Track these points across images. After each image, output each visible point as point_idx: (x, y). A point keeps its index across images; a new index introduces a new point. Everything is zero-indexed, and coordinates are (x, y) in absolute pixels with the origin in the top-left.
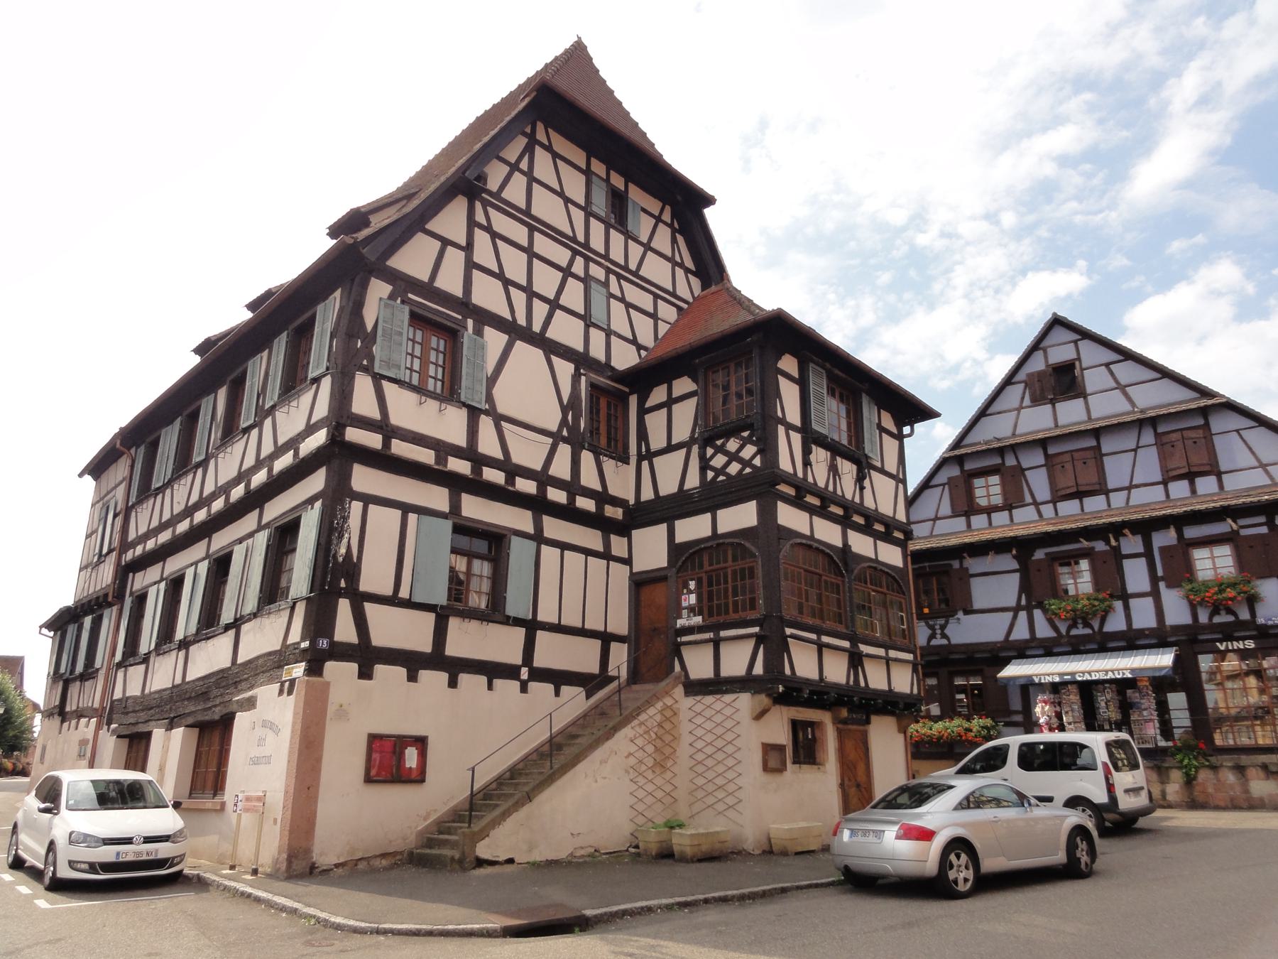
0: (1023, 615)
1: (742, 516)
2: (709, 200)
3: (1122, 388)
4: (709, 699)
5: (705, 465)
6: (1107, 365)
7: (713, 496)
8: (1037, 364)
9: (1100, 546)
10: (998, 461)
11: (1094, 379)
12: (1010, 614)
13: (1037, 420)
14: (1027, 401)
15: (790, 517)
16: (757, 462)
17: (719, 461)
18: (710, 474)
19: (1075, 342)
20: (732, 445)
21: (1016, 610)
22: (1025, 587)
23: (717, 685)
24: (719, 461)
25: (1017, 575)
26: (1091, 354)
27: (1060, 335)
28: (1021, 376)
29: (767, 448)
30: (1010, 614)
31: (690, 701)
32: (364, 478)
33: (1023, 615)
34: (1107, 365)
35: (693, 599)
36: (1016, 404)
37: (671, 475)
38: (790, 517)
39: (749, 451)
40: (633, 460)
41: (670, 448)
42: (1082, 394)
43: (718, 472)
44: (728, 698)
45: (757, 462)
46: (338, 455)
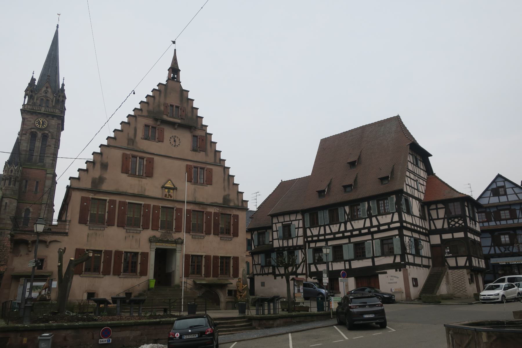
0: (493, 248)
1: (461, 235)
2: (431, 155)
3: (516, 194)
4: (456, 270)
5: (449, 224)
6: (512, 188)
7: (452, 230)
8: (494, 186)
9: (512, 232)
10: (484, 210)
11: (509, 191)
12: (489, 248)
13: (494, 200)
14: (492, 195)
15: (470, 235)
16: (463, 224)
17: (453, 223)
18: (451, 226)
19: (504, 181)
20: (456, 220)
21: (491, 247)
22: (493, 241)
23: (457, 267)
24: (453, 223)
25: (491, 239)
26: (507, 185)
27: (500, 179)
28: (490, 188)
29: (465, 222)
30: (489, 248)
31: (450, 271)
32: (405, 232)
33: (493, 248)
34: (512, 188)
35: (448, 250)
36: (489, 196)
37: (439, 224)
38: (470, 235)
39: (461, 222)
40: (428, 221)
41: (438, 219)
42: (505, 194)
43: (453, 225)
44: (461, 270)
45: (463, 224)
46: (400, 229)
